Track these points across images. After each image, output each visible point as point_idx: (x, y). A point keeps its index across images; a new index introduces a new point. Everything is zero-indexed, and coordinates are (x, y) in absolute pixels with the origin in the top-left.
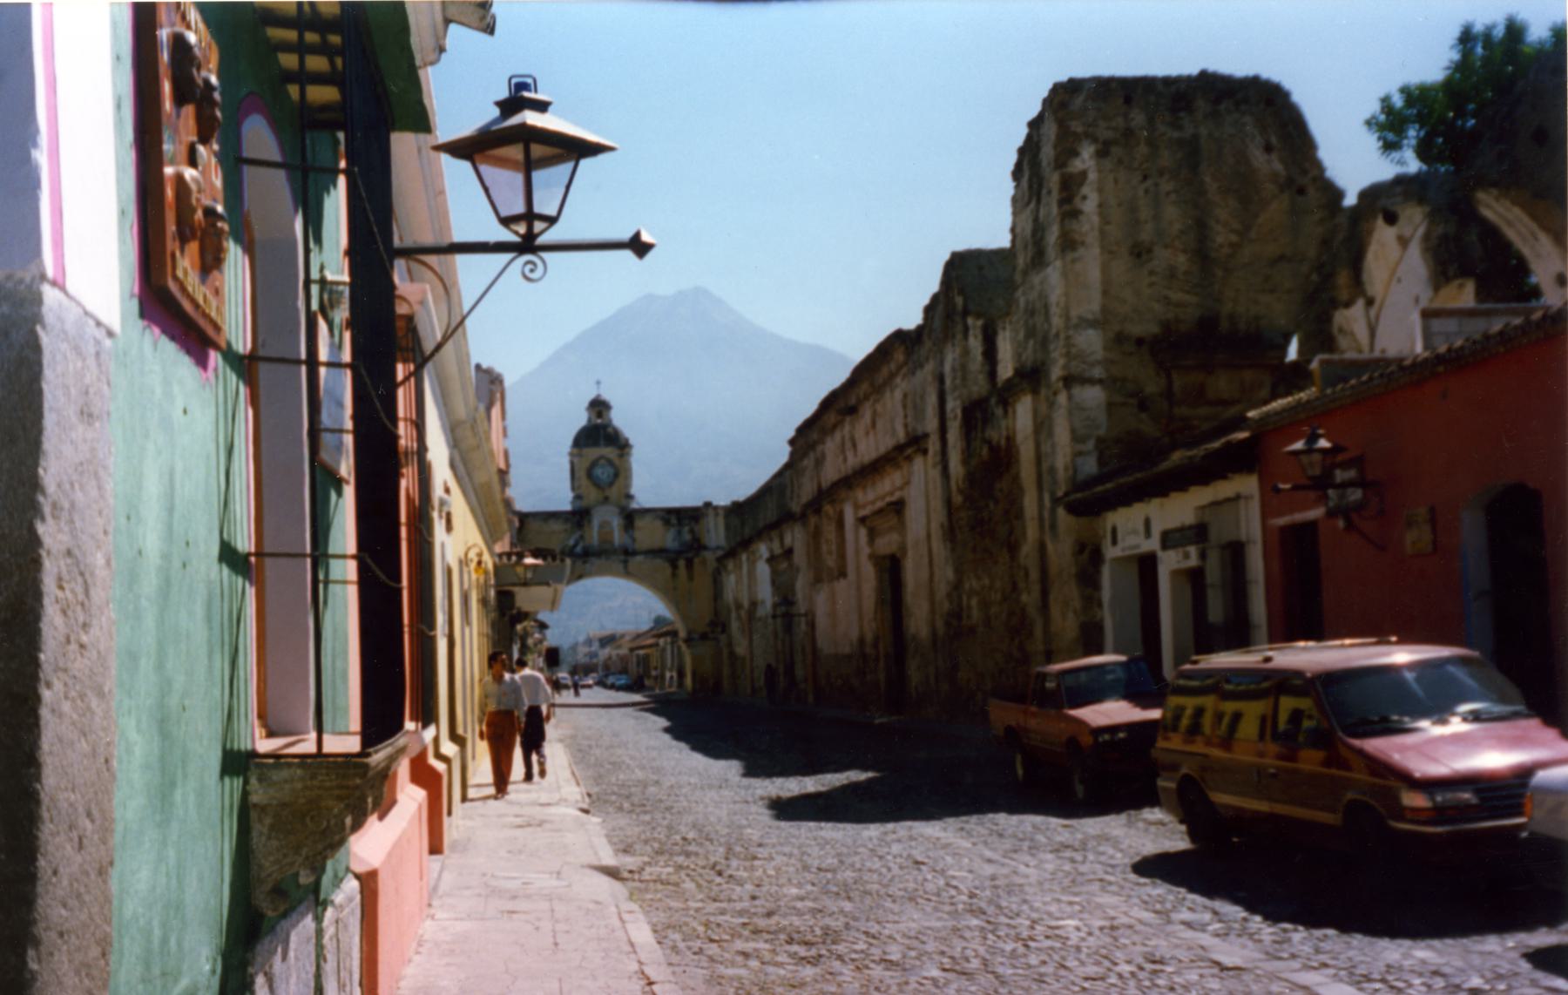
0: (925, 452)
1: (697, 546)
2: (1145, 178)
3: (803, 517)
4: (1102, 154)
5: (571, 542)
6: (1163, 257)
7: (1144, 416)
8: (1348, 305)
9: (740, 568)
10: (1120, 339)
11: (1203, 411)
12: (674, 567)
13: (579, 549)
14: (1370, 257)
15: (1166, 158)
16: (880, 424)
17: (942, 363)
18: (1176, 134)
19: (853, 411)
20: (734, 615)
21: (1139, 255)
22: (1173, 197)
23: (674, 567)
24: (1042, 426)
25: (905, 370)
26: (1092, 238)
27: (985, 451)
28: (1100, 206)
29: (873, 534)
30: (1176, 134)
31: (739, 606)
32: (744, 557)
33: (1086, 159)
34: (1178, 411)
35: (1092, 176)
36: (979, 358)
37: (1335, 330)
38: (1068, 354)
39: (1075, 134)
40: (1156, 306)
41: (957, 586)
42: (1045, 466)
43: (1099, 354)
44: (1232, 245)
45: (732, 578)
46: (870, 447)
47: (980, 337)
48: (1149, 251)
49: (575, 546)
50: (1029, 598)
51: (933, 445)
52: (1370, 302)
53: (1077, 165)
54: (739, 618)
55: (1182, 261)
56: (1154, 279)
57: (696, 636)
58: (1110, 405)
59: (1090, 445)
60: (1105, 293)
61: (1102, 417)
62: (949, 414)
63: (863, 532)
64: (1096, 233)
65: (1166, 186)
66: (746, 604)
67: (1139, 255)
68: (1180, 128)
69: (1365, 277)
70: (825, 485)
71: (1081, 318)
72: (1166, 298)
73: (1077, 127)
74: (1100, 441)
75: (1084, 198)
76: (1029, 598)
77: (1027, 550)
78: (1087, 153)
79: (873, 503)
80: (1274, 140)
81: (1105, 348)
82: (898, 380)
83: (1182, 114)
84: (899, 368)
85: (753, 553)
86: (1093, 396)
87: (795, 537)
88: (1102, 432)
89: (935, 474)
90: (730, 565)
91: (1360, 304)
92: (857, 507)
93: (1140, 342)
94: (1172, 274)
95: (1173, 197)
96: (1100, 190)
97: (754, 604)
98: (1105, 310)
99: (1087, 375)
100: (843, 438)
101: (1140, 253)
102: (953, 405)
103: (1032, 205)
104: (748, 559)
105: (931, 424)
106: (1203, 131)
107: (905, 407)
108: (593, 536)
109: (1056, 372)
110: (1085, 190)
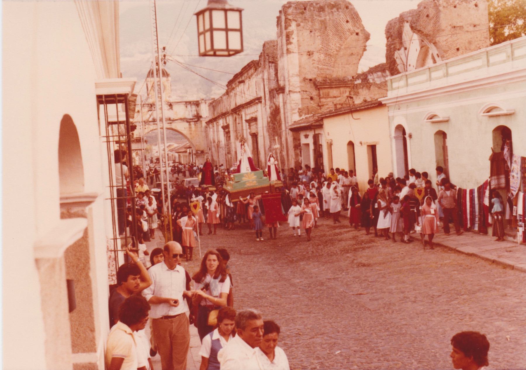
0: (261, 102)
1: (198, 117)
2: (311, 32)
3: (232, 114)
4: (298, 25)
5: (148, 116)
6: (316, 56)
7: (312, 102)
8: (399, 50)
9: (214, 126)
10: (305, 79)
11: (329, 100)
12: (190, 125)
13: (151, 119)
14: (404, 35)
15: (317, 25)
16: (250, 88)
17: (263, 75)
18: (320, 19)
19: (243, 82)
20: (213, 144)
21: (309, 55)
22: (319, 37)
23: (190, 125)
24: (285, 103)
25: (255, 74)
26: (296, 50)
27: (274, 107)
28: (298, 41)
29: (250, 126)
30: (320, 19)
31: (214, 142)
32: (215, 123)
33: (293, 26)
34: (322, 100)
35: (295, 32)
36: (274, 76)
37: (395, 58)
38: (289, 84)
39: (290, 20)
40: (316, 70)
41: (270, 147)
42: (286, 115)
43: (298, 84)
44: (337, 51)
45: (211, 130)
46: (249, 96)
47: (274, 69)
48: (312, 54)
49: (149, 118)
50: (284, 153)
51: (263, 101)
52: (406, 49)
53: (290, 29)
54: (214, 146)
55: (322, 56)
56: (314, 62)
57: (199, 152)
58: (302, 99)
59: (296, 111)
60: (300, 67)
61: (299, 102)
62: (266, 93)
63: (247, 124)
64: (297, 49)
65: (317, 34)
66: (216, 141)
67: (309, 55)
68: (320, 17)
69: (403, 41)
70: (238, 104)
71: (293, 74)
72: (318, 67)
73: (290, 17)
74: (299, 109)
75: (293, 39)
76: (284, 153)
77: (283, 139)
78: (293, 25)
79: (250, 114)
80: (349, 19)
81: (300, 82)
82: (254, 76)
83: (321, 13)
84: (254, 72)
85: (218, 122)
86: (296, 97)
87: (230, 120)
88: (300, 106)
89: (264, 109)
90: (211, 125)
91: (403, 49)
92: (246, 115)
93: (311, 80)
94: (319, 61)
95: (319, 37)
96: (298, 36)
97: (219, 142)
98: (300, 71)
99: (295, 90)
100: (241, 90)
101: (310, 54)
102: (267, 90)
103: (281, 37)
104: (216, 124)
105: (262, 94)
106: (328, 18)
107: (256, 85)
108: (157, 114)
109: (287, 90)
110: (293, 36)
